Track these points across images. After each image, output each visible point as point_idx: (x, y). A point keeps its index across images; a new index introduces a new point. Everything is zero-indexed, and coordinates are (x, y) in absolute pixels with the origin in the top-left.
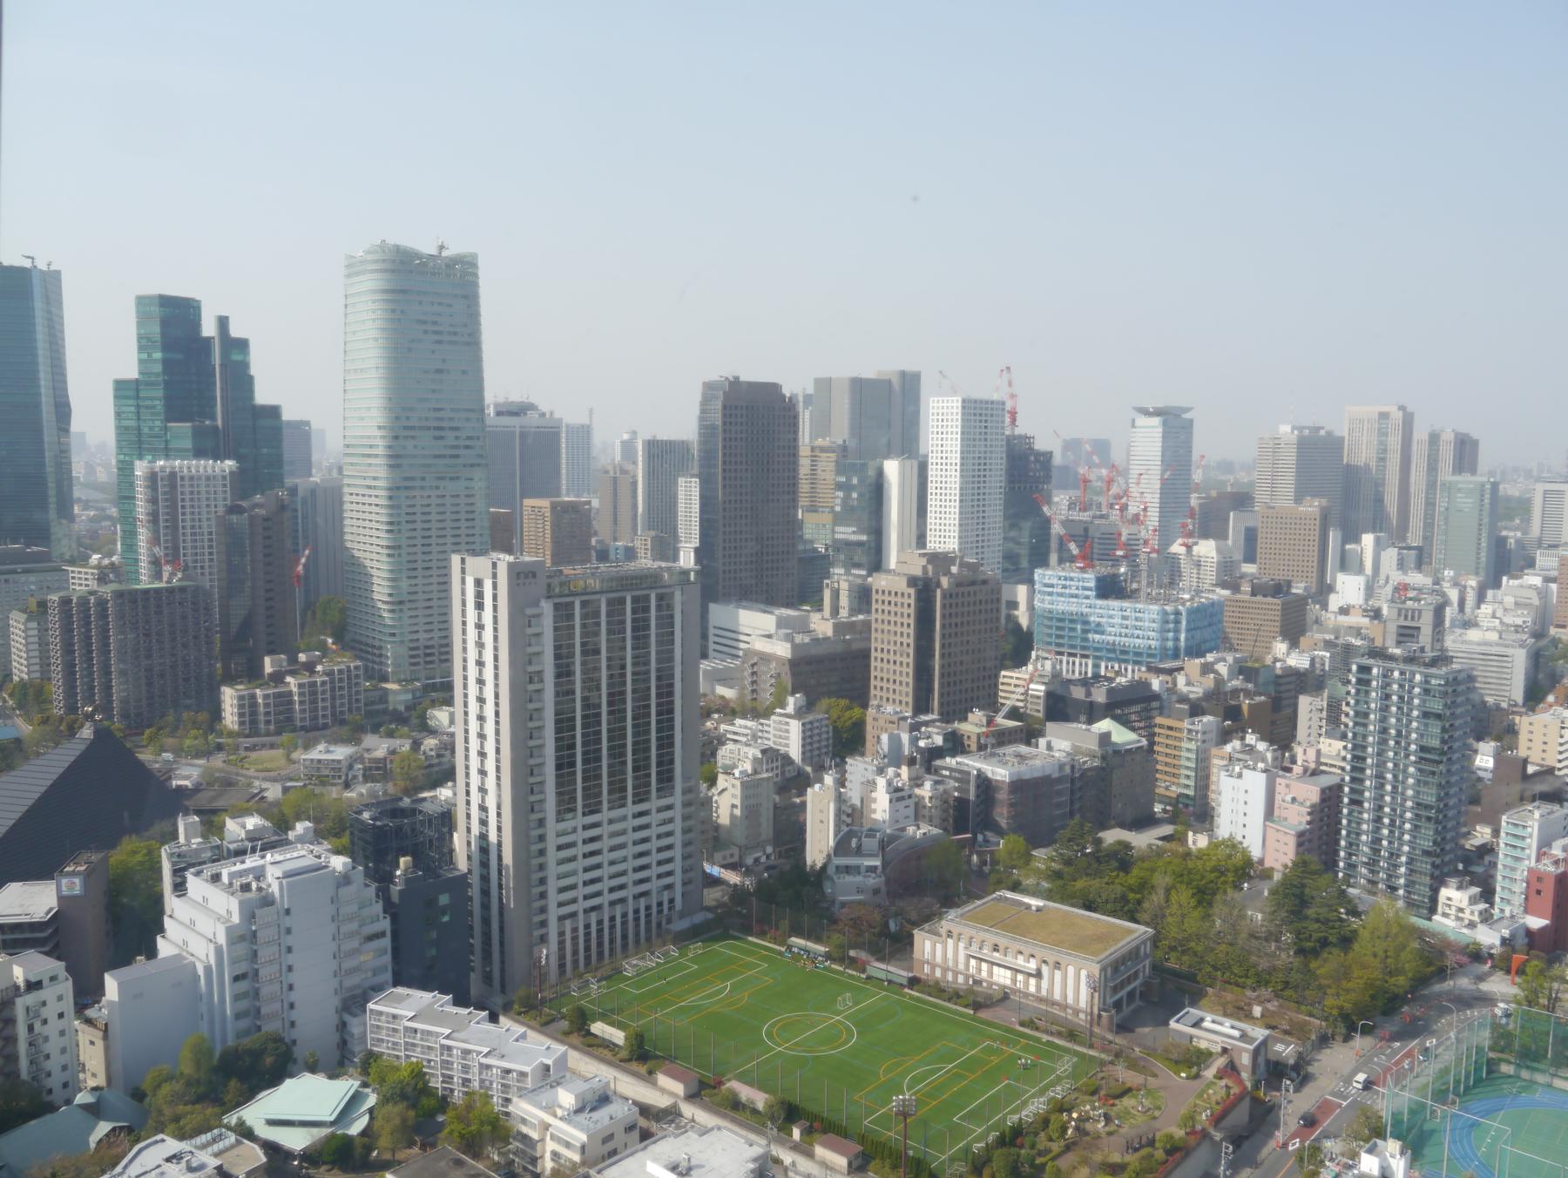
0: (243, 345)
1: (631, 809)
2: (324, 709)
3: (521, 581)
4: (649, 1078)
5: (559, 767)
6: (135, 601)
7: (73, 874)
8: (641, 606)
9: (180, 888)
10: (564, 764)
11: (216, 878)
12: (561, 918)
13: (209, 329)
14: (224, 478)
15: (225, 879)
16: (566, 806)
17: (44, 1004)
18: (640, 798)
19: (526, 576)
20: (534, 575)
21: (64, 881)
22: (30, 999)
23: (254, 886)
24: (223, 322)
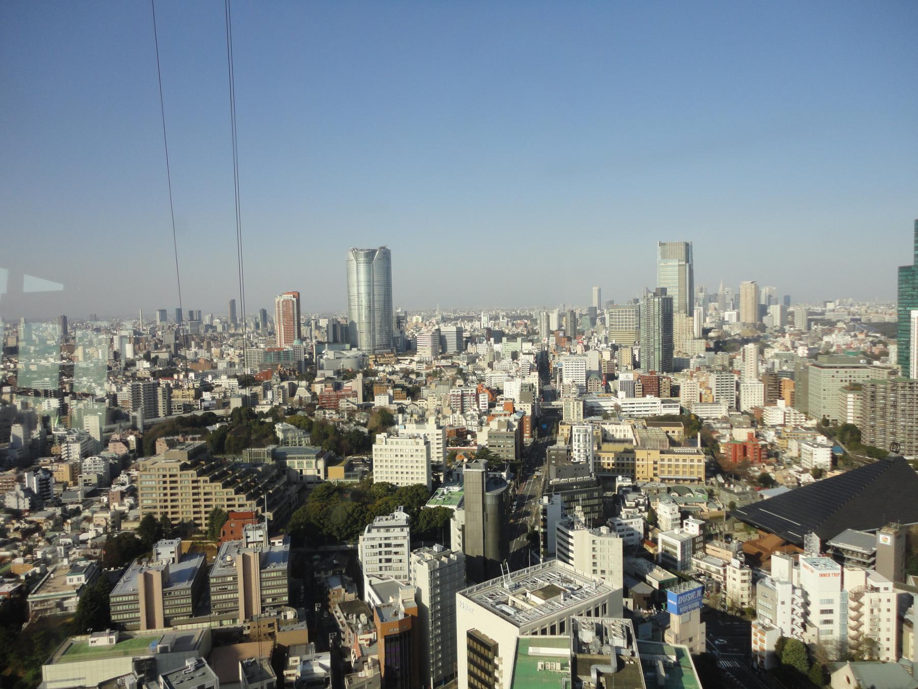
7: (887, 534)
17: (880, 600)
22: (874, 596)
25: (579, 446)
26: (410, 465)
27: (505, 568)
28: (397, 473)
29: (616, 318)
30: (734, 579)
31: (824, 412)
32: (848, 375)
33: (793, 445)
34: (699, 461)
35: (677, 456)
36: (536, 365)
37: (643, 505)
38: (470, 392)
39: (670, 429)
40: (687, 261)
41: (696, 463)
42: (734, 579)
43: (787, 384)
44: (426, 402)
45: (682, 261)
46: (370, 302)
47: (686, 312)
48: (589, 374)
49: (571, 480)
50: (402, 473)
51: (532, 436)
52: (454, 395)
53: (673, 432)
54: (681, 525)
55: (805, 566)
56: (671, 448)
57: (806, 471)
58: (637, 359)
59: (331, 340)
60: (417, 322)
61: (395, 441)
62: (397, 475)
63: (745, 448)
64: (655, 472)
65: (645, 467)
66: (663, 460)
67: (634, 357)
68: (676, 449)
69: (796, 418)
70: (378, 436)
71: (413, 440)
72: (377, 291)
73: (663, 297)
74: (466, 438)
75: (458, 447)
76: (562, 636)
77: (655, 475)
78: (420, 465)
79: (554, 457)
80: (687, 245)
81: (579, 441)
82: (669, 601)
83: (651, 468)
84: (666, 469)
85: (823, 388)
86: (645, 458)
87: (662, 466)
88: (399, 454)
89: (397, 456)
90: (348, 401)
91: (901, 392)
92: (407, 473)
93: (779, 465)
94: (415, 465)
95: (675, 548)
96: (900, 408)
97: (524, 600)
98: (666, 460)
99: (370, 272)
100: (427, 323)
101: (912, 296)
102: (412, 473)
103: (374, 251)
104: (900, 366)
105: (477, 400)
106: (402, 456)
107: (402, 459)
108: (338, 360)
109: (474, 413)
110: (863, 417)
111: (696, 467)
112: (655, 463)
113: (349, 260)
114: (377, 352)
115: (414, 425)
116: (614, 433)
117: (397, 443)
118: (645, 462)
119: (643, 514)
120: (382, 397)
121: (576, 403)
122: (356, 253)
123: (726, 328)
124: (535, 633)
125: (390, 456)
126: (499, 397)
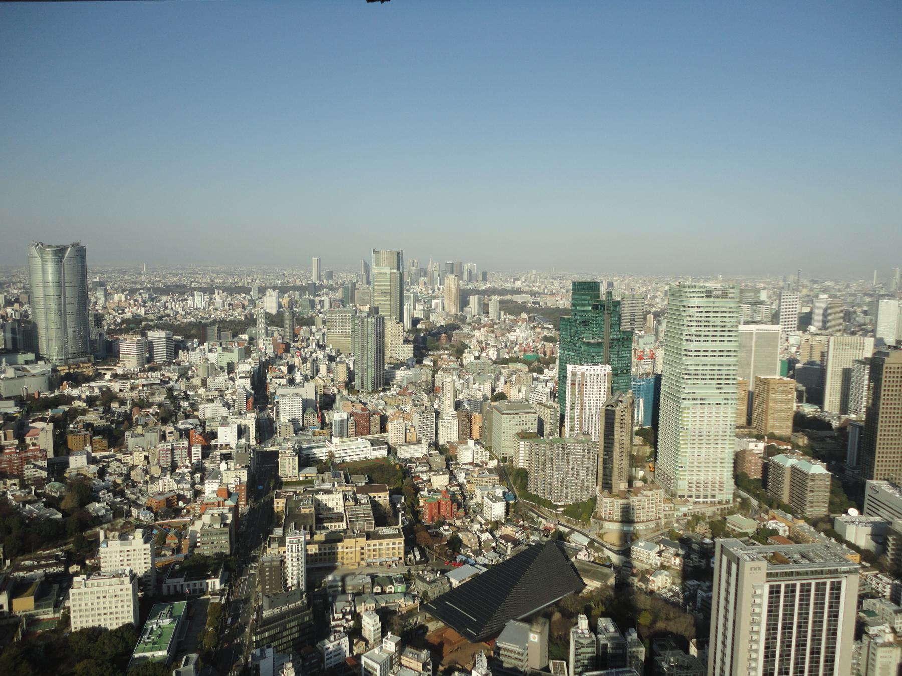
3: (752, 572)
7: (535, 633)
13: (603, 296)
20: (760, 568)
25: (291, 556)
26: (114, 605)
28: (99, 615)
29: (333, 323)
31: (503, 450)
32: (521, 419)
34: (400, 543)
35: (381, 541)
36: (253, 392)
37: (350, 613)
38: (181, 446)
39: (377, 495)
40: (399, 269)
41: (397, 545)
43: (476, 418)
44: (131, 457)
45: (394, 269)
46: (60, 305)
47: (396, 319)
48: (306, 404)
49: (284, 608)
50: (105, 614)
51: (247, 504)
52: (163, 450)
53: (380, 497)
54: (382, 641)
56: (377, 529)
58: (352, 369)
59: (9, 346)
60: (119, 301)
61: (95, 582)
62: (99, 617)
63: (439, 503)
64: (362, 556)
65: (354, 553)
66: (369, 546)
67: (349, 368)
68: (382, 531)
69: (483, 455)
70: (75, 579)
71: (116, 579)
72: (69, 292)
73: (376, 316)
74: (178, 504)
75: (169, 520)
77: (362, 559)
78: (125, 604)
79: (267, 569)
80: (399, 253)
81: (292, 551)
83: (358, 554)
84: (372, 553)
85: (502, 431)
86: (353, 545)
87: (369, 551)
88: (101, 595)
89: (98, 598)
90: (35, 466)
91: (556, 451)
92: (111, 614)
93: (466, 518)
94: (120, 604)
96: (555, 464)
98: (372, 545)
99: (59, 272)
100: (132, 302)
101: (570, 342)
102: (117, 613)
103: (65, 248)
104: (559, 405)
105: (190, 454)
106: (104, 597)
107: (104, 600)
108: (20, 380)
109: (187, 470)
110: (529, 460)
111: (397, 549)
112: (362, 548)
113: (31, 257)
114: (70, 361)
115: (118, 542)
116: (327, 502)
117: (99, 585)
118: (353, 549)
120: (79, 457)
121: (291, 458)
122: (40, 249)
125: (88, 599)
126: (213, 442)
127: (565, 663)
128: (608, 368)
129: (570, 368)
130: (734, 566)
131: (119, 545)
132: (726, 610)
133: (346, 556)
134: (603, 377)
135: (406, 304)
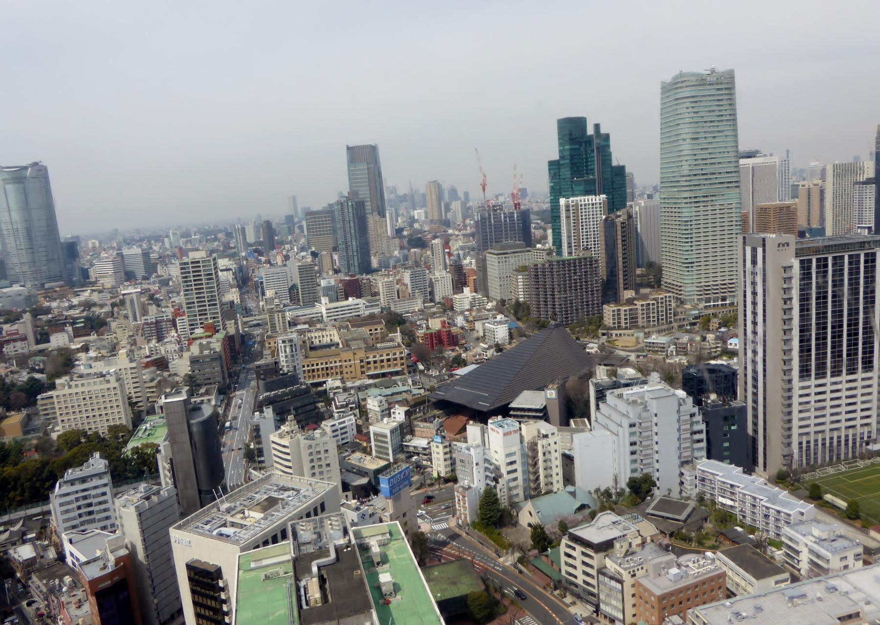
0: (607, 137)
1: (844, 377)
2: (654, 317)
4: (865, 528)
5: (801, 351)
6: (564, 265)
7: (552, 389)
8: (854, 261)
9: (601, 396)
10: (805, 350)
11: (620, 396)
12: (800, 435)
13: (590, 131)
14: (600, 204)
15: (625, 397)
16: (805, 372)
17: (549, 445)
18: (852, 371)
19: (783, 245)
20: (788, 244)
21: (548, 392)
22: (544, 442)
23: (639, 401)
24: (597, 127)
27: (217, 492)
30: (438, 453)
33: (478, 325)
42: (438, 453)
55: (492, 429)
57: (490, 347)
65: (353, 366)
66: (368, 358)
76: (283, 542)
81: (285, 351)
82: (382, 485)
86: (352, 358)
87: (369, 363)
95: (386, 437)
97: (242, 518)
102: (106, 414)
104: (555, 247)
117: (83, 385)
118: (352, 362)
119: (355, 412)
121: (280, 314)
123: (416, 226)
124: (258, 547)
127: (586, 420)
128: (604, 196)
129: (562, 201)
130: (760, 251)
131: (103, 365)
132: (755, 323)
133: (345, 370)
134: (598, 206)
135: (387, 212)
